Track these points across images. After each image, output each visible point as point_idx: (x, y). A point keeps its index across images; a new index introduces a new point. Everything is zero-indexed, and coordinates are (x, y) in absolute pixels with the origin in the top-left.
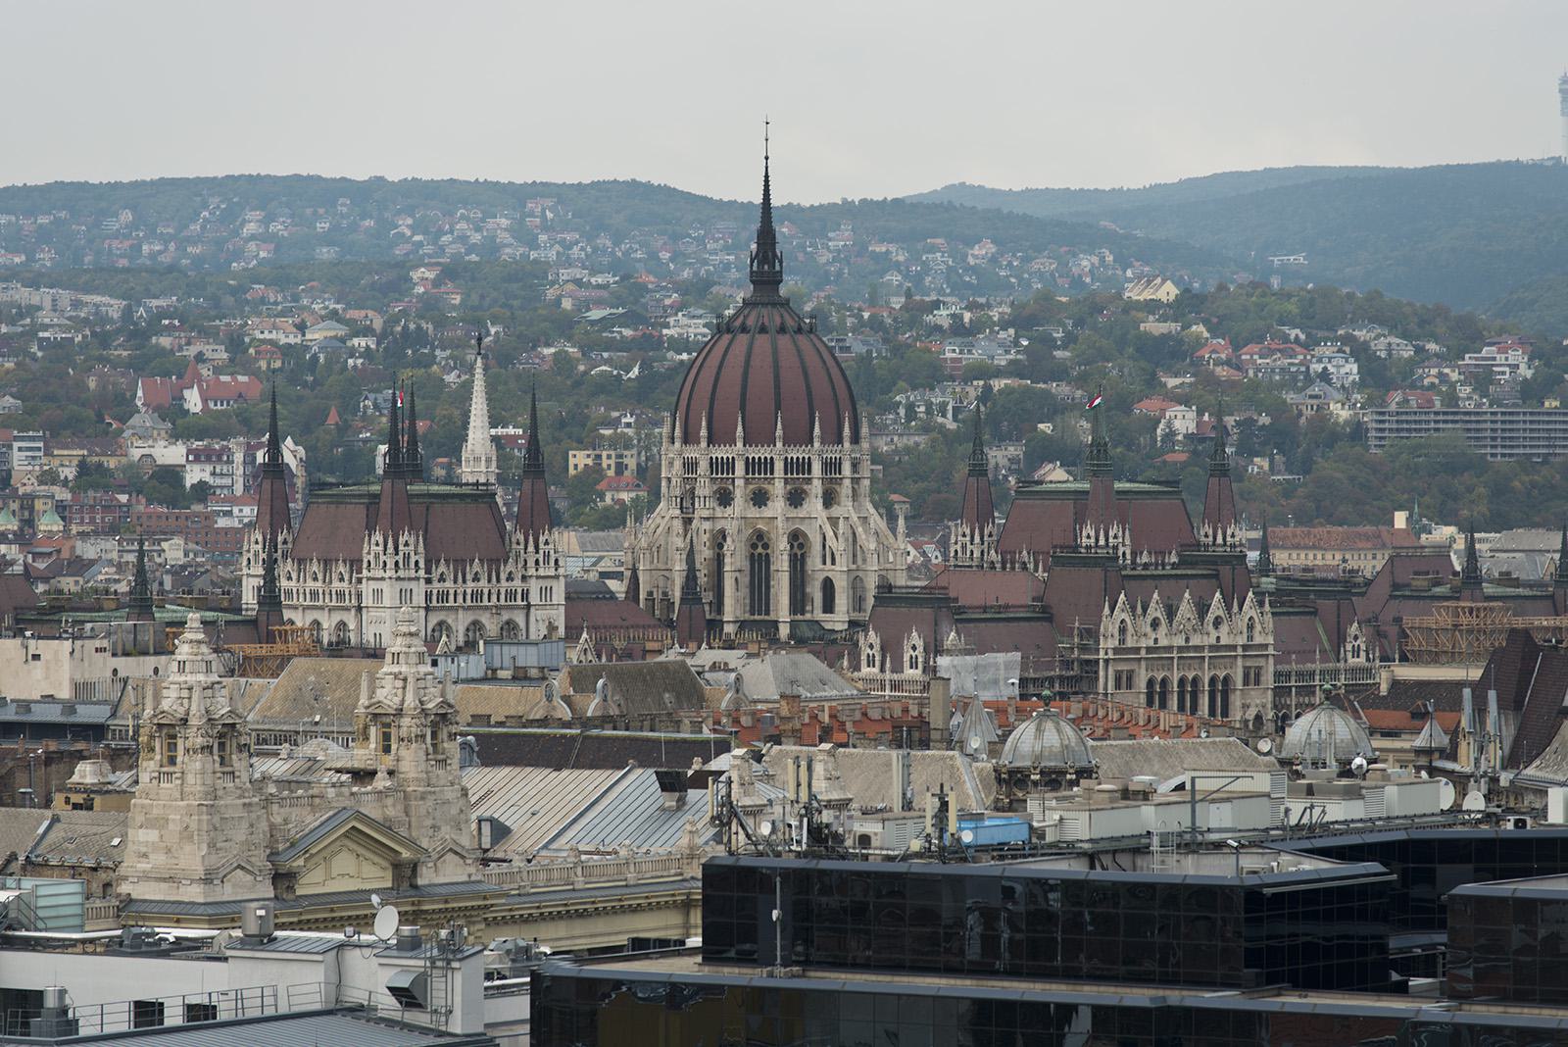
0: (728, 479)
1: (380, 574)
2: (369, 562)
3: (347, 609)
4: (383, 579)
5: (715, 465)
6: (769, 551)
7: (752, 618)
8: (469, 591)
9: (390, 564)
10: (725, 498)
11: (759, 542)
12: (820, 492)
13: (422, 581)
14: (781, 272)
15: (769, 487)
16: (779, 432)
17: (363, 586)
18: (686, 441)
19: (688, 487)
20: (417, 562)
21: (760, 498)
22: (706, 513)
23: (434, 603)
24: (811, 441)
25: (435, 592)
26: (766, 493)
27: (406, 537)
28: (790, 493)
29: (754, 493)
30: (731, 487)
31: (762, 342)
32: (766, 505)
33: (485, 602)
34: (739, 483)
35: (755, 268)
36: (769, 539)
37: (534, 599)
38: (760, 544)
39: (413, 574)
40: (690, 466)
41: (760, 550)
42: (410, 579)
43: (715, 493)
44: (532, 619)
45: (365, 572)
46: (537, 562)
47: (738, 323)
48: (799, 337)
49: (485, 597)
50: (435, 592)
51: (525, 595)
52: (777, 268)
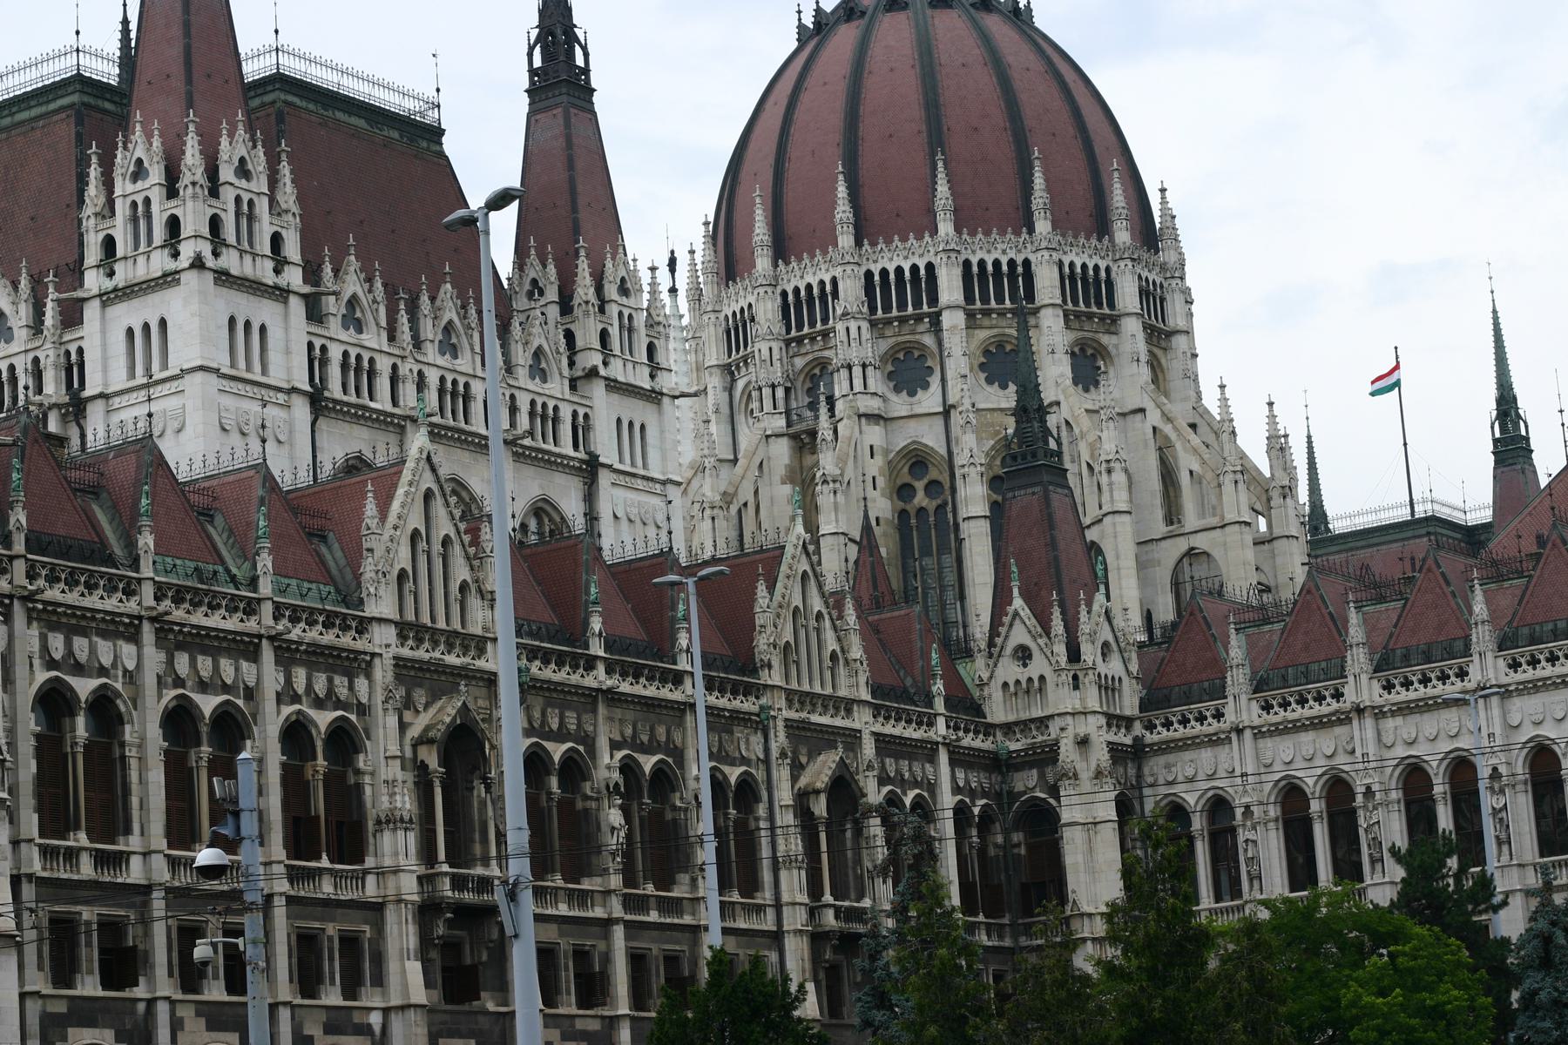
2: (109, 244)
4: (168, 279)
9: (194, 218)
10: (909, 370)
13: (297, 307)
19: (799, 362)
22: (872, 405)
29: (986, 352)
30: (928, 340)
34: (953, 320)
37: (605, 445)
39: (264, 271)
40: (805, 312)
43: (884, 359)
45: (94, 281)
51: (582, 429)
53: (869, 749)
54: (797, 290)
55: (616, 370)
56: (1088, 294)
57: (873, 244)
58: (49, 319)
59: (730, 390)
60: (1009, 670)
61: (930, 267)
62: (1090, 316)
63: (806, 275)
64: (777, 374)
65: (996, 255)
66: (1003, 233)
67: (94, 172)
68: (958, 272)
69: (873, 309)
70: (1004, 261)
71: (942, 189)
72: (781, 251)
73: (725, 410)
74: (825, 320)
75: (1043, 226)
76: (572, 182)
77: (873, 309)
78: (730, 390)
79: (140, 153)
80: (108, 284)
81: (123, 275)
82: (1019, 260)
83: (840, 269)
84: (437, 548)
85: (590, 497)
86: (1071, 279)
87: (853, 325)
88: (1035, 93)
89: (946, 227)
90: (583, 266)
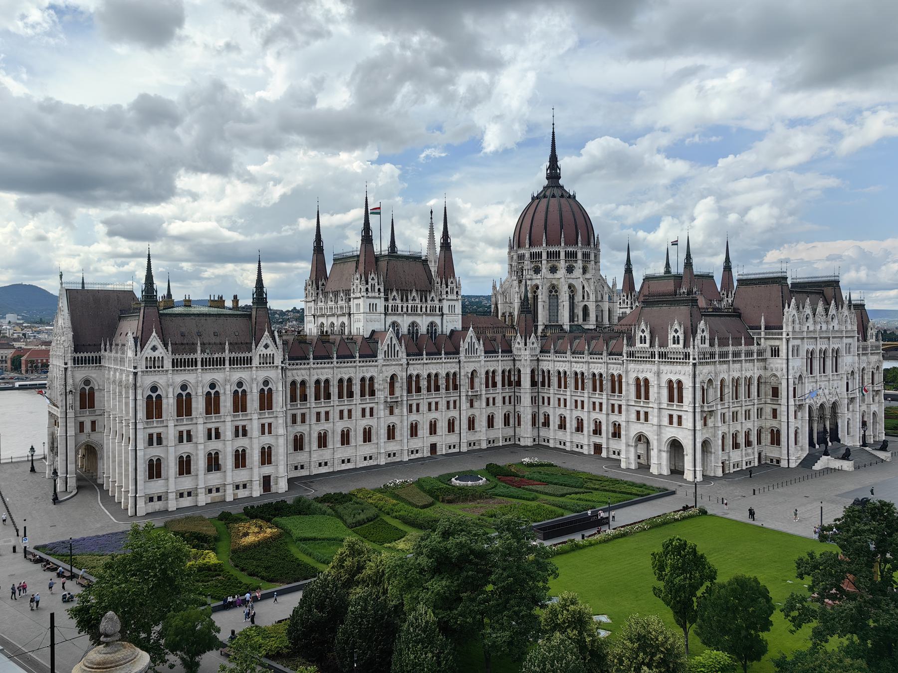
3: (344, 315)
5: (532, 256)
8: (410, 306)
9: (363, 289)
10: (537, 270)
12: (581, 266)
13: (383, 299)
21: (553, 270)
25: (390, 305)
37: (446, 311)
40: (521, 257)
42: (374, 298)
44: (444, 321)
46: (447, 292)
50: (390, 305)
51: (441, 309)
53: (483, 363)
55: (449, 297)
56: (571, 256)
60: (517, 346)
63: (521, 252)
72: (519, 247)
75: (563, 244)
83: (526, 252)
86: (567, 254)
88: (568, 216)
89: (544, 245)
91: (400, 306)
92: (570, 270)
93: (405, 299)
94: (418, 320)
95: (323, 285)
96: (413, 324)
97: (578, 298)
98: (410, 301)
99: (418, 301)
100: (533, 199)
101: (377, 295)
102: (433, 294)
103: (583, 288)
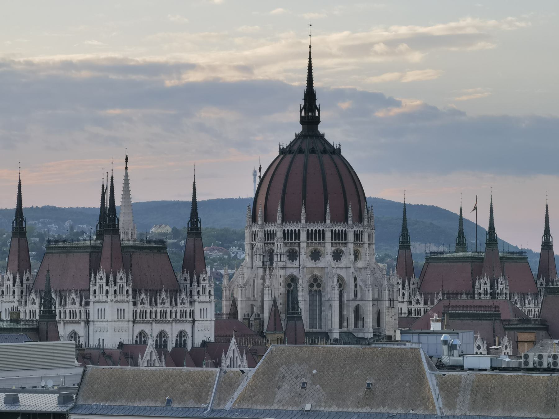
0: (295, 243)
1: (104, 298)
2: (95, 291)
3: (78, 322)
4: (106, 302)
5: (286, 235)
6: (321, 289)
7: (311, 330)
8: (159, 311)
9: (111, 291)
10: (293, 255)
11: (316, 283)
12: (352, 252)
13: (131, 303)
14: (319, 117)
15: (322, 249)
16: (328, 215)
17: (91, 307)
18: (266, 219)
19: (267, 249)
20: (127, 291)
21: (315, 255)
22: (281, 264)
23: (138, 318)
24: (346, 220)
25: (138, 311)
26: (319, 252)
27: (121, 274)
28: (334, 252)
29: (312, 252)
30: (297, 249)
31: (313, 159)
32: (319, 260)
33: (168, 318)
34: (303, 245)
35: (303, 114)
36: (321, 281)
37: (197, 316)
38: (315, 284)
39: (125, 298)
40: (269, 236)
41: (315, 288)
42: (123, 302)
43: (286, 252)
45: (92, 297)
47: (296, 147)
48: (334, 157)
49: (168, 315)
50: (138, 311)
51: (192, 314)
52: (317, 114)
54: (268, 231)
55: (202, 298)
57: (286, 223)
58: (83, 303)
59: (252, 250)
61: (299, 230)
62: (339, 243)
63: (270, 228)
64: (261, 252)
65: (316, 228)
66: (318, 223)
67: (93, 275)
68: (305, 233)
69: (284, 240)
70: (318, 230)
71: (303, 211)
73: (250, 255)
74: (273, 240)
75: (328, 222)
76: (194, 255)
77: (284, 240)
78: (252, 250)
79: (101, 274)
80: (95, 299)
81: (97, 299)
82: (321, 229)
84: (153, 362)
85: (193, 327)
87: (279, 244)
89: (303, 221)
90: (195, 277)
91: (148, 311)
92: (337, 256)
93: (153, 303)
94: (167, 328)
95: (28, 280)
96: (162, 334)
97: (349, 294)
98: (159, 305)
99: (167, 304)
100: (282, 151)
101: (125, 298)
102: (183, 296)
103: (355, 279)
